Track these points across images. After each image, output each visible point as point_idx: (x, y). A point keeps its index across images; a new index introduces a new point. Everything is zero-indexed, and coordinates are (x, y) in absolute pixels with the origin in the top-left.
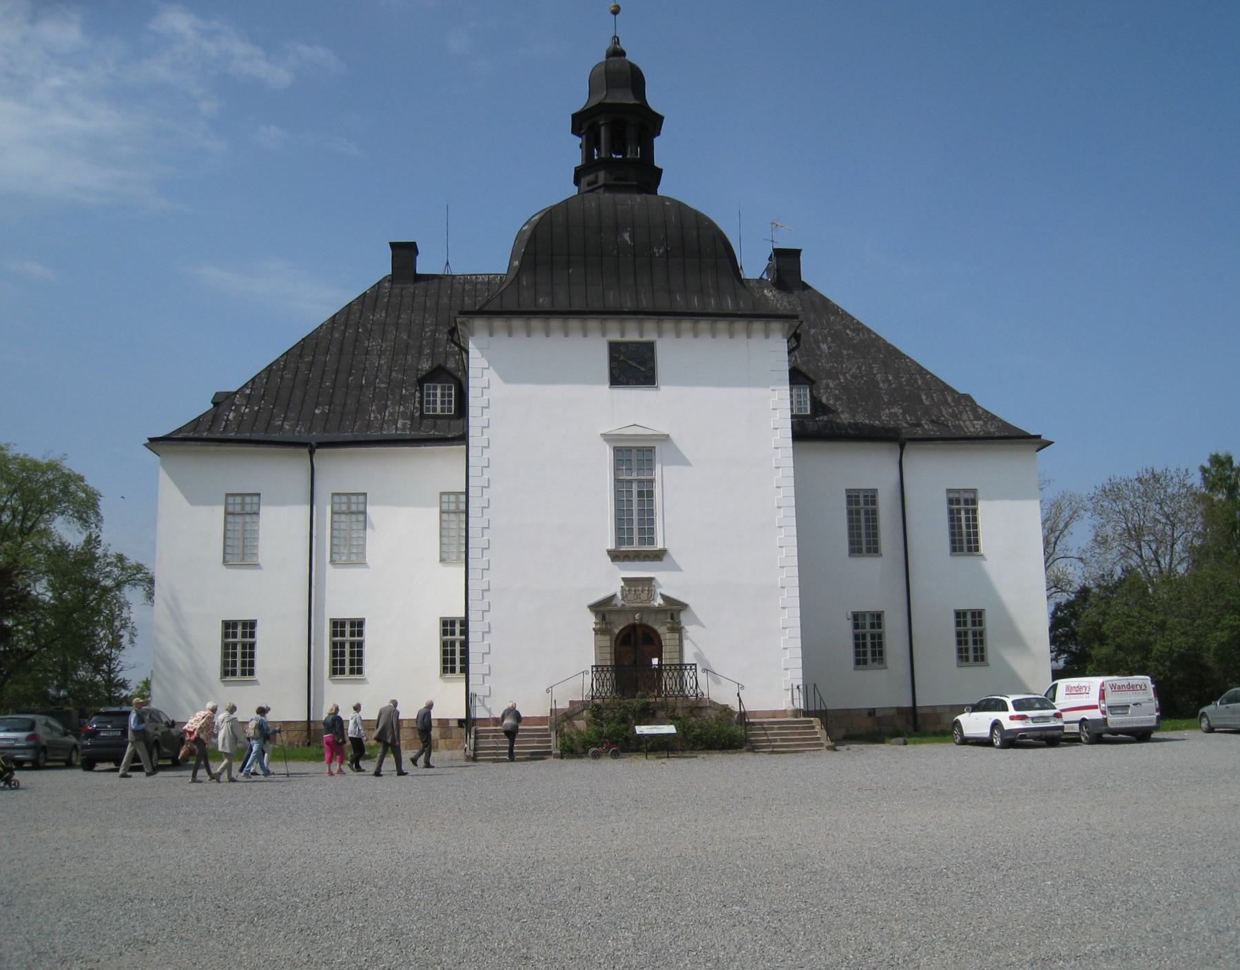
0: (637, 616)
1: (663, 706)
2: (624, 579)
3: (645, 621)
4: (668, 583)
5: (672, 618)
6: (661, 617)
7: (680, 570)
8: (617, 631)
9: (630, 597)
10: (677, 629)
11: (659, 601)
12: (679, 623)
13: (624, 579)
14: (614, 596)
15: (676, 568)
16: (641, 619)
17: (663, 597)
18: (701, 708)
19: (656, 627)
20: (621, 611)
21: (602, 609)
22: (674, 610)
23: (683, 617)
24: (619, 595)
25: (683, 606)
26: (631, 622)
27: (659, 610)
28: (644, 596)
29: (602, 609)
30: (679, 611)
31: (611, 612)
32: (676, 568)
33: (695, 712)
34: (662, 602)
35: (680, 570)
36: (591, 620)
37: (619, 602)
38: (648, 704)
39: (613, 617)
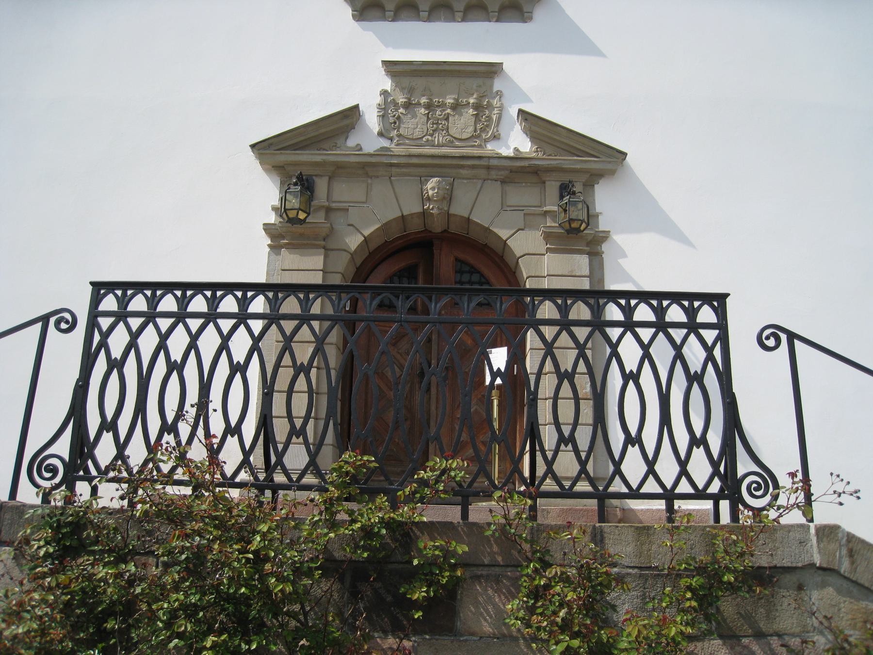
0: (432, 183)
1: (517, 555)
2: (392, 68)
3: (460, 209)
4: (543, 80)
5: (565, 189)
6: (523, 196)
7: (596, 52)
8: (354, 242)
9: (415, 124)
10: (580, 234)
11: (516, 142)
12: (591, 217)
13: (392, 68)
14: (349, 117)
15: (578, 43)
16: (448, 197)
17: (532, 122)
18: (763, 578)
19: (503, 234)
20: (369, 168)
21: (306, 162)
22: (572, 172)
23: (607, 202)
24: (372, 119)
25: (607, 160)
26: (412, 207)
27: (517, 172)
28: (462, 124)
29: (306, 162)
30: (593, 178)
31: (339, 171)
32: (578, 43)
33: (728, 606)
34: (525, 146)
35: (596, 52)
36: (263, 196)
37: (369, 137)
38: (404, 534)
39: (345, 192)
